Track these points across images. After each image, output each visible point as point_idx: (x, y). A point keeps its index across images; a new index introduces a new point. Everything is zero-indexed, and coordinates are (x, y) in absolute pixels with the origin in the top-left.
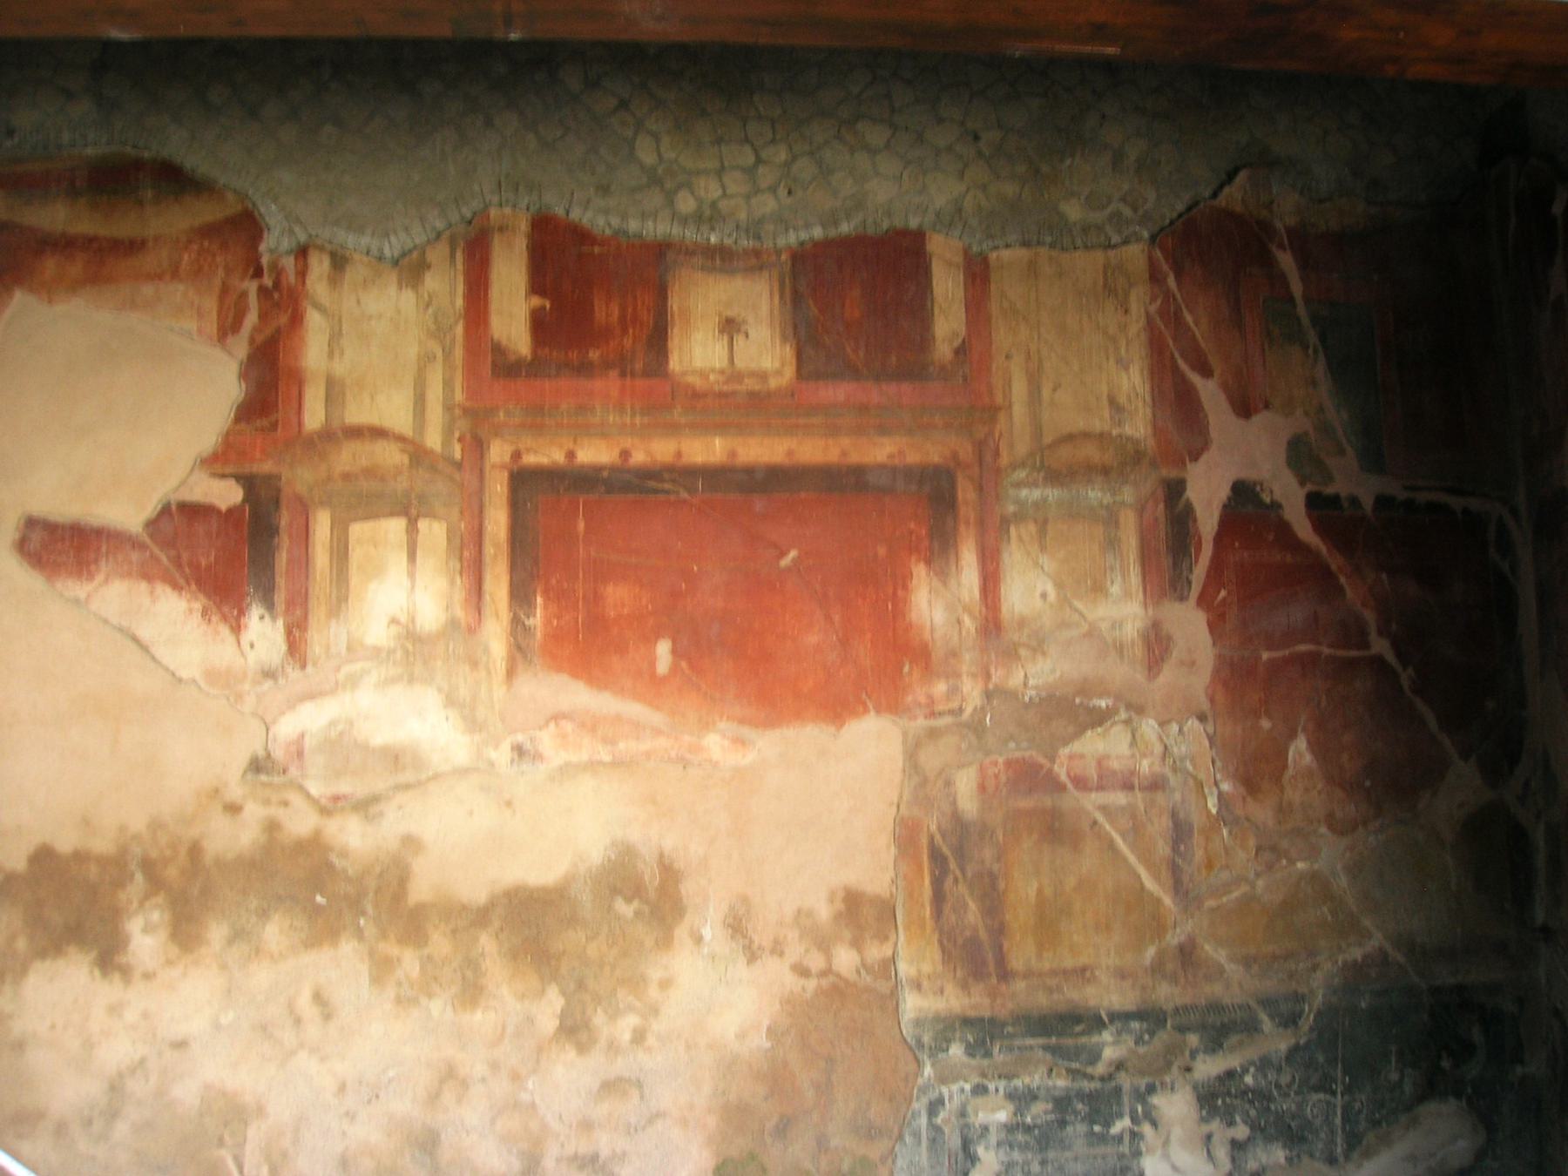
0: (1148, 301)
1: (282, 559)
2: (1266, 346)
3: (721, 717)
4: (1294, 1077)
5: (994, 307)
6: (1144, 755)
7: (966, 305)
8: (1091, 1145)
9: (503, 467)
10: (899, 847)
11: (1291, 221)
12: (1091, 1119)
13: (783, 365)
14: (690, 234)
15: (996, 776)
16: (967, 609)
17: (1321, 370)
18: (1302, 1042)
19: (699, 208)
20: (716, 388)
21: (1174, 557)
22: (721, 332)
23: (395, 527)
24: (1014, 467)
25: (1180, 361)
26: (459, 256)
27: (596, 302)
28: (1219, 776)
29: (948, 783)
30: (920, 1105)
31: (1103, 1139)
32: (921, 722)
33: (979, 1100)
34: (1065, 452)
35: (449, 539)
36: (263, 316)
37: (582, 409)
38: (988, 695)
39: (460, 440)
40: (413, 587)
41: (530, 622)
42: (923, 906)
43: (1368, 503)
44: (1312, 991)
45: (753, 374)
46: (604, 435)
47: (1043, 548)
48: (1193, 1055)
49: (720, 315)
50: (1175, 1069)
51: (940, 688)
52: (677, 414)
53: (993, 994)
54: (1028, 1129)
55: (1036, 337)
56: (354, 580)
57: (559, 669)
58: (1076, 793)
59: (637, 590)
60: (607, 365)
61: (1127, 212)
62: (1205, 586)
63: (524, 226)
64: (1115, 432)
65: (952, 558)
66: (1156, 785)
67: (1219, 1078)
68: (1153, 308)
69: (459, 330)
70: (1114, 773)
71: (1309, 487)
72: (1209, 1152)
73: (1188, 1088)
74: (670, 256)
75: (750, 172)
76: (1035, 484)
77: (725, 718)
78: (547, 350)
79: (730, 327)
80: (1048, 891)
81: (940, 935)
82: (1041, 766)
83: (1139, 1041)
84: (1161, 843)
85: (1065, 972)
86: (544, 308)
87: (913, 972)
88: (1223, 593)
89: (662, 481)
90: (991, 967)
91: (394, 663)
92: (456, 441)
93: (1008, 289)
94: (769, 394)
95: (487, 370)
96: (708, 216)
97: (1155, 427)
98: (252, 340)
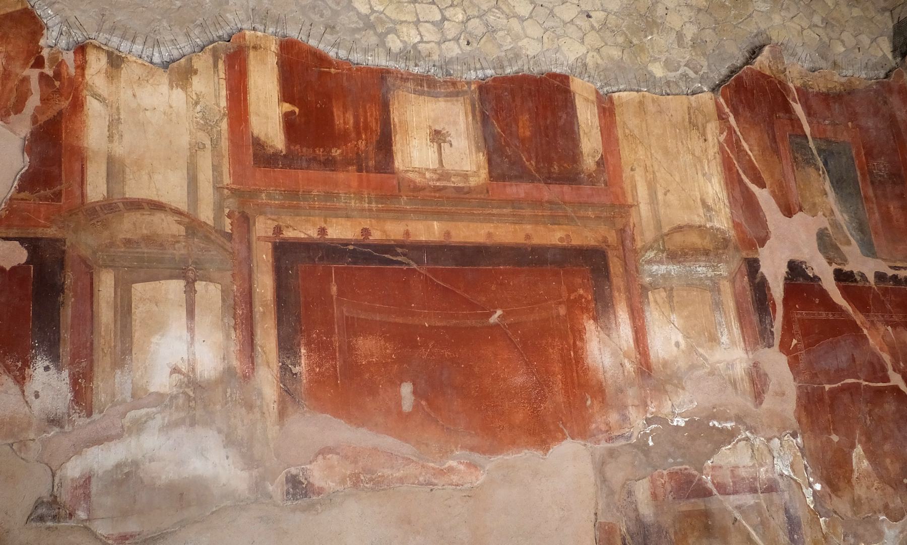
0: (718, 131)
1: (67, 314)
2: (795, 168)
3: (456, 447)
5: (620, 133)
6: (761, 465)
7: (601, 131)
9: (266, 239)
11: (798, 83)
13: (479, 168)
14: (401, 66)
15: (663, 485)
16: (626, 355)
17: (828, 186)
19: (405, 48)
20: (431, 183)
21: (759, 316)
22: (432, 141)
23: (175, 287)
24: (646, 249)
25: (743, 177)
26: (221, 65)
27: (335, 110)
28: (811, 479)
29: (630, 493)
34: (678, 238)
35: (223, 300)
36: (43, 100)
37: (329, 196)
38: (649, 422)
39: (229, 216)
40: (192, 338)
41: (296, 370)
43: (871, 278)
45: (457, 175)
46: (348, 217)
47: (672, 309)
49: (430, 127)
51: (614, 417)
52: (403, 202)
55: (649, 156)
56: (137, 335)
57: (324, 411)
58: (721, 497)
59: (383, 342)
60: (347, 162)
61: (691, 74)
62: (783, 336)
63: (274, 47)
64: (708, 226)
65: (612, 317)
66: (771, 488)
68: (722, 138)
69: (224, 125)
70: (743, 479)
71: (835, 266)
74: (390, 80)
75: (438, 25)
76: (661, 262)
77: (459, 449)
78: (298, 147)
79: (438, 137)
82: (694, 476)
84: (781, 533)
86: (293, 112)
88: (795, 342)
89: (397, 255)
91: (177, 408)
92: (226, 218)
93: (627, 120)
94: (470, 191)
95: (250, 160)
96: (410, 54)
97: (733, 221)
98: (35, 119)
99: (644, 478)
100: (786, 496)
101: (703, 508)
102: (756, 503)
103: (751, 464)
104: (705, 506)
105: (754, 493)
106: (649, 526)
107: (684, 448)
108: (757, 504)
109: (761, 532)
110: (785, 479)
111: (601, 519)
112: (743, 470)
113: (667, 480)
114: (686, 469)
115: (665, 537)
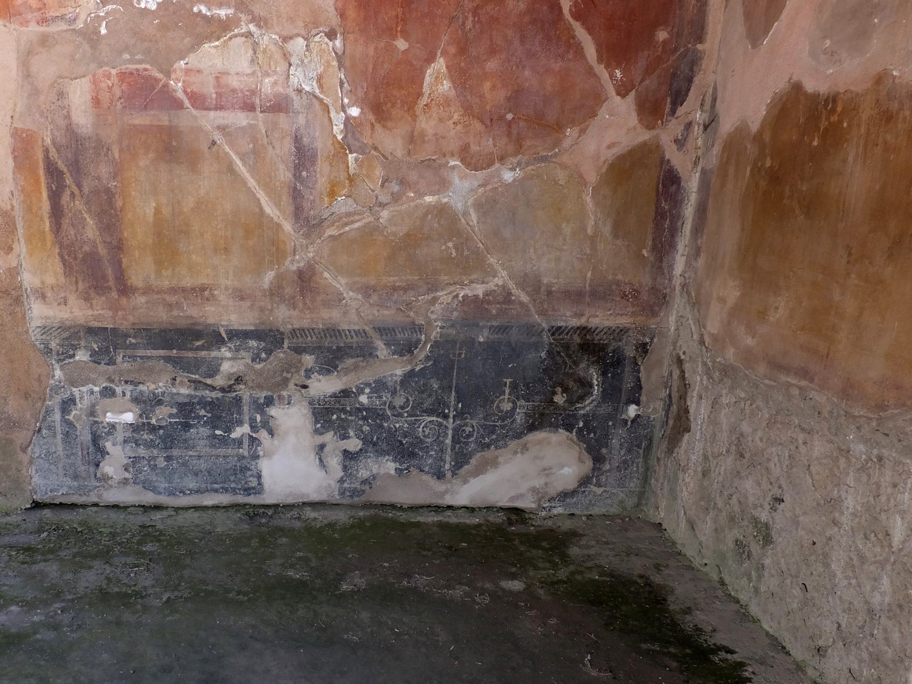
4: (408, 400)
6: (267, 74)
8: (213, 446)
10: (15, 158)
12: (213, 423)
15: (110, 88)
28: (346, 101)
29: (61, 95)
30: (54, 403)
31: (224, 441)
32: (34, 29)
33: (108, 401)
42: (42, 219)
44: (429, 323)
48: (308, 373)
50: (291, 386)
53: (114, 307)
54: (153, 429)
66: (279, 106)
70: (234, 91)
73: (305, 404)
80: (166, 211)
81: (60, 248)
82: (157, 80)
83: (256, 358)
84: (282, 167)
85: (184, 290)
87: (37, 283)
90: (111, 283)
99: (84, 76)
100: (301, 120)
101: (166, 123)
102: (252, 124)
103: (249, 71)
104: (170, 121)
105: (252, 111)
106: (85, 139)
107: (151, 41)
108: (251, 126)
109: (251, 163)
110: (305, 97)
111: (19, 125)
112: (236, 77)
113: (116, 82)
114: (146, 70)
115: (106, 155)
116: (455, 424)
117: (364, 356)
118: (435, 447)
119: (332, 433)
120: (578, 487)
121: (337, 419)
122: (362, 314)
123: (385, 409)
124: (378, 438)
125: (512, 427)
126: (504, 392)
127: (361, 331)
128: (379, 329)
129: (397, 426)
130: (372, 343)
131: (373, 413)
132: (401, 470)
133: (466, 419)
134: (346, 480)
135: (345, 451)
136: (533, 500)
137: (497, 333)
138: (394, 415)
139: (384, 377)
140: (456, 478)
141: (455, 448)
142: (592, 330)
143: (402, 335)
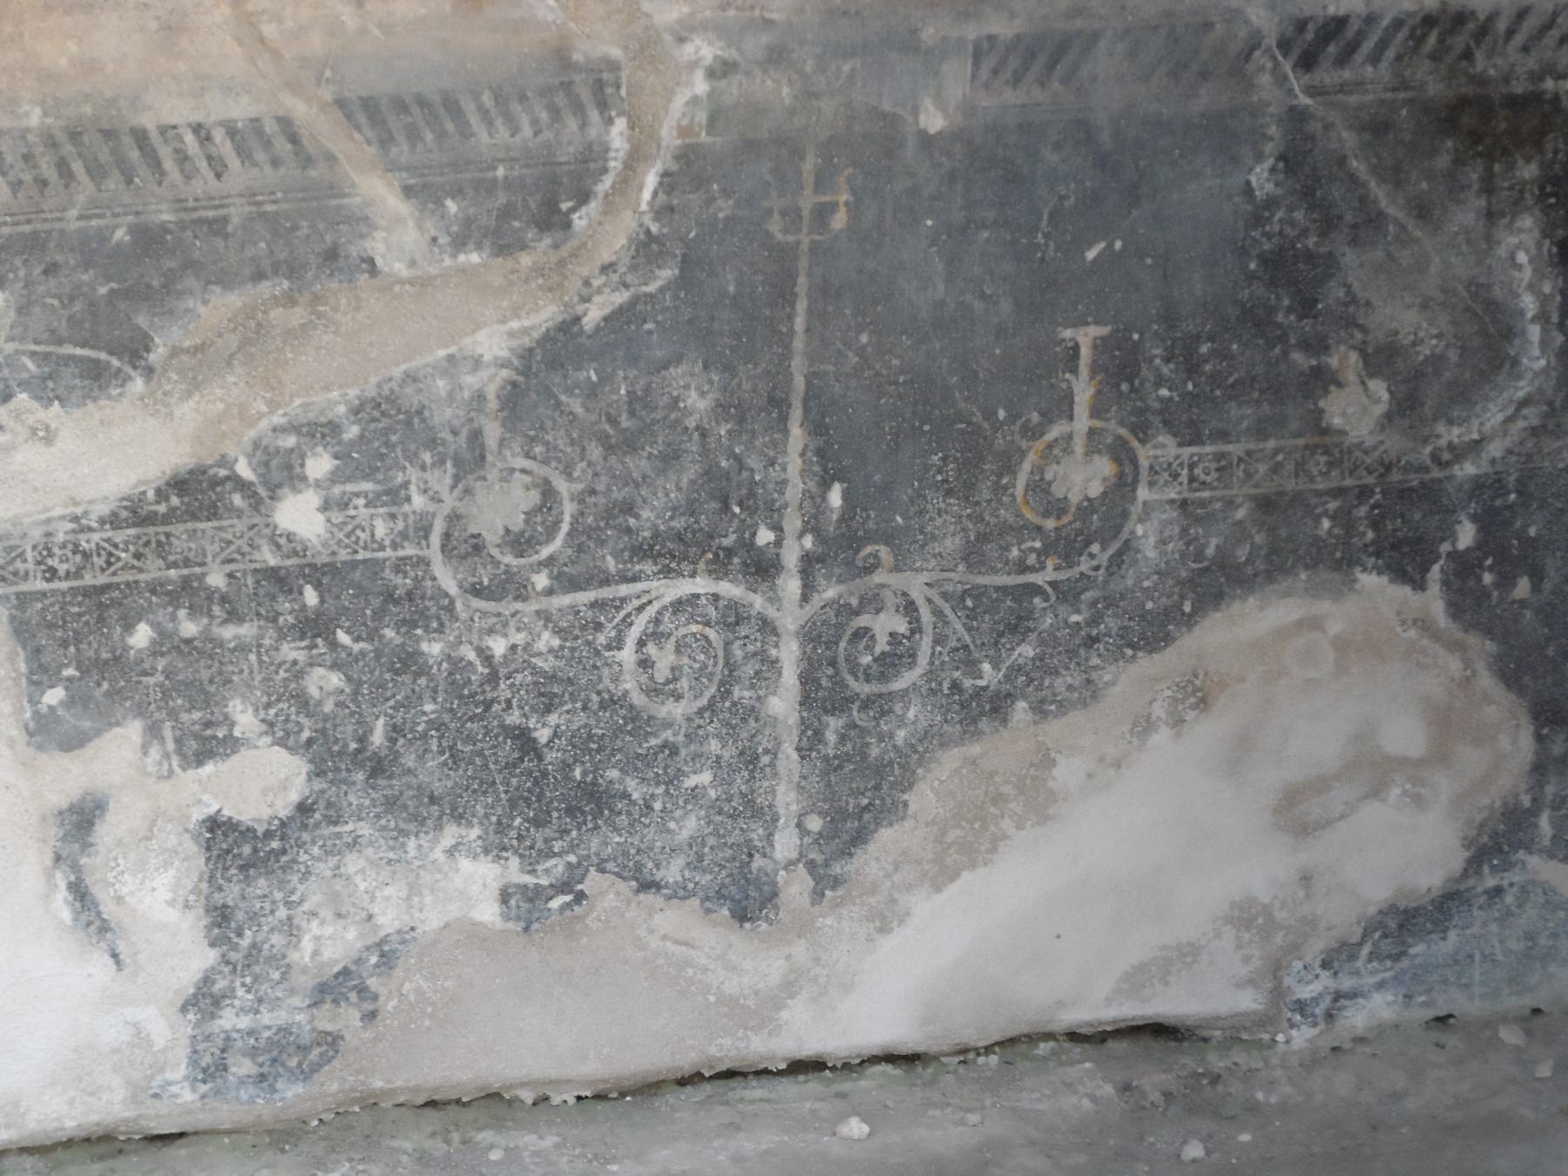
18: (593, 315)
44: (648, 49)
67: (134, 513)
72: (80, 893)
116: (817, 601)
117: (293, 270)
118: (714, 746)
119: (133, 730)
120: (1465, 874)
121: (155, 650)
122: (268, 30)
123: (424, 562)
124: (395, 731)
125: (1116, 586)
126: (1068, 398)
127: (270, 127)
128: (370, 106)
129: (498, 646)
130: (334, 190)
131: (362, 592)
132: (534, 896)
133: (869, 569)
134: (230, 993)
135: (214, 824)
136: (1244, 972)
137: (1017, 80)
138: (477, 591)
139: (411, 377)
140: (837, 905)
141: (818, 736)
142: (1501, 26)
143: (503, 133)
